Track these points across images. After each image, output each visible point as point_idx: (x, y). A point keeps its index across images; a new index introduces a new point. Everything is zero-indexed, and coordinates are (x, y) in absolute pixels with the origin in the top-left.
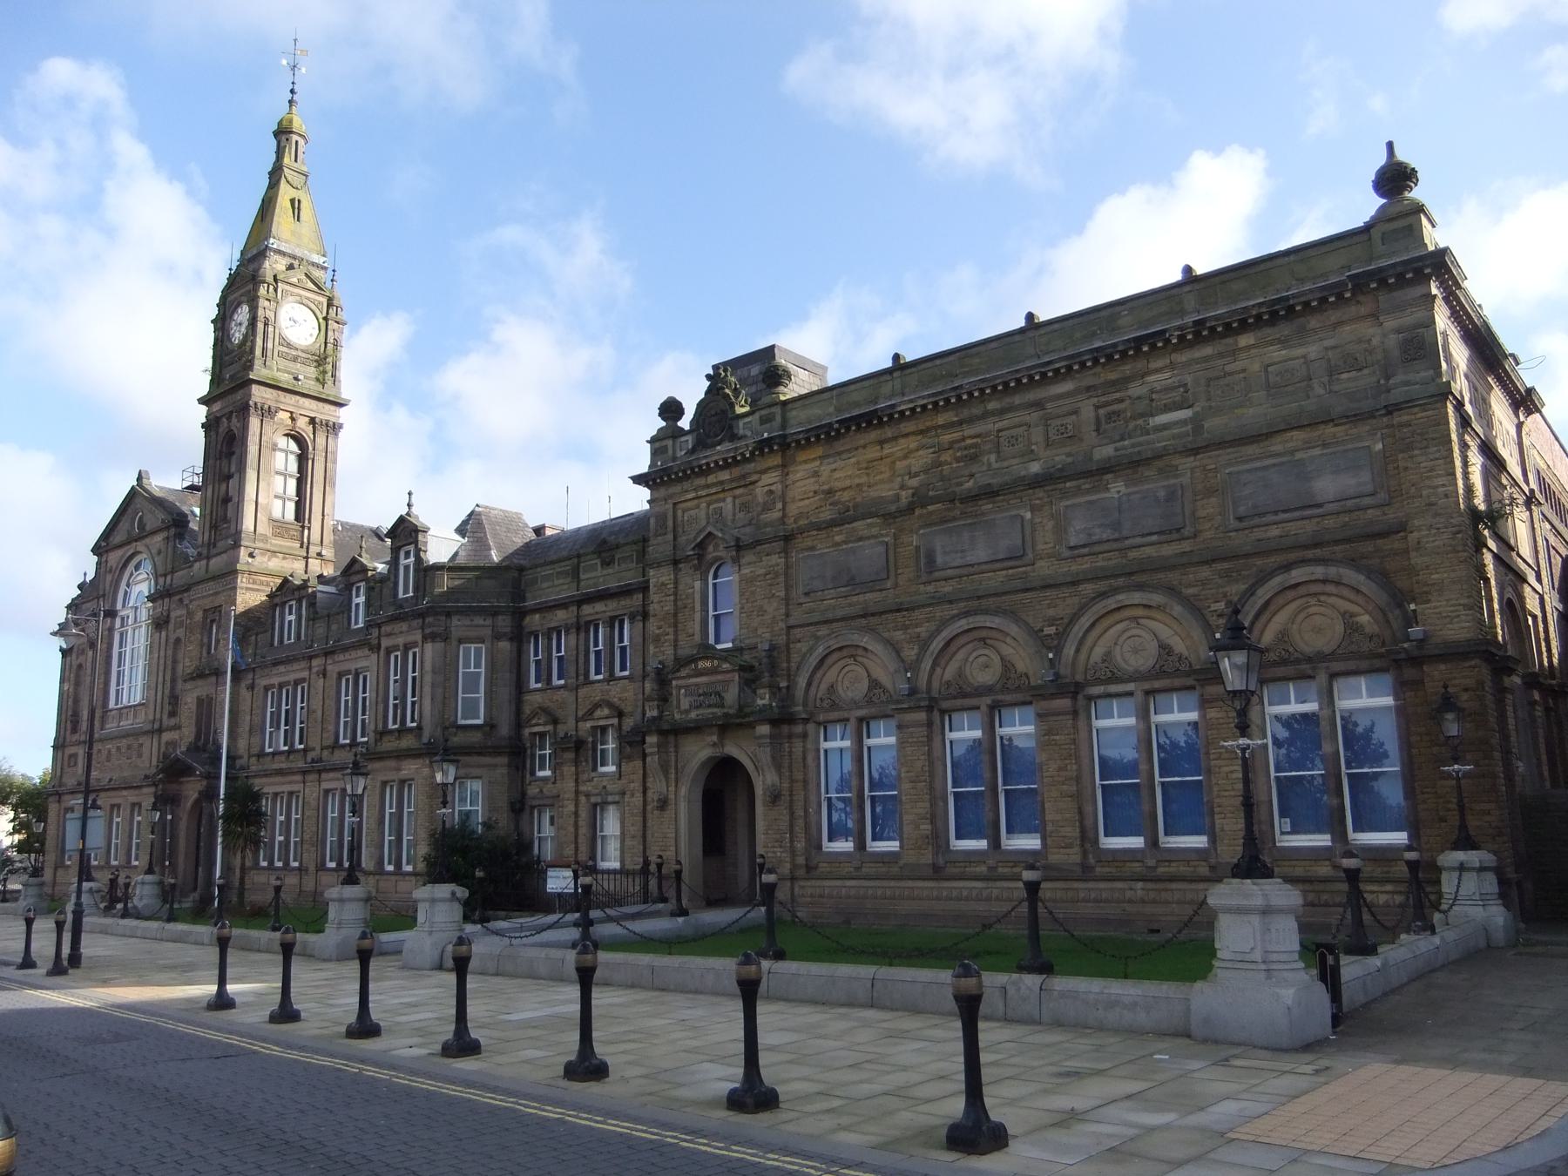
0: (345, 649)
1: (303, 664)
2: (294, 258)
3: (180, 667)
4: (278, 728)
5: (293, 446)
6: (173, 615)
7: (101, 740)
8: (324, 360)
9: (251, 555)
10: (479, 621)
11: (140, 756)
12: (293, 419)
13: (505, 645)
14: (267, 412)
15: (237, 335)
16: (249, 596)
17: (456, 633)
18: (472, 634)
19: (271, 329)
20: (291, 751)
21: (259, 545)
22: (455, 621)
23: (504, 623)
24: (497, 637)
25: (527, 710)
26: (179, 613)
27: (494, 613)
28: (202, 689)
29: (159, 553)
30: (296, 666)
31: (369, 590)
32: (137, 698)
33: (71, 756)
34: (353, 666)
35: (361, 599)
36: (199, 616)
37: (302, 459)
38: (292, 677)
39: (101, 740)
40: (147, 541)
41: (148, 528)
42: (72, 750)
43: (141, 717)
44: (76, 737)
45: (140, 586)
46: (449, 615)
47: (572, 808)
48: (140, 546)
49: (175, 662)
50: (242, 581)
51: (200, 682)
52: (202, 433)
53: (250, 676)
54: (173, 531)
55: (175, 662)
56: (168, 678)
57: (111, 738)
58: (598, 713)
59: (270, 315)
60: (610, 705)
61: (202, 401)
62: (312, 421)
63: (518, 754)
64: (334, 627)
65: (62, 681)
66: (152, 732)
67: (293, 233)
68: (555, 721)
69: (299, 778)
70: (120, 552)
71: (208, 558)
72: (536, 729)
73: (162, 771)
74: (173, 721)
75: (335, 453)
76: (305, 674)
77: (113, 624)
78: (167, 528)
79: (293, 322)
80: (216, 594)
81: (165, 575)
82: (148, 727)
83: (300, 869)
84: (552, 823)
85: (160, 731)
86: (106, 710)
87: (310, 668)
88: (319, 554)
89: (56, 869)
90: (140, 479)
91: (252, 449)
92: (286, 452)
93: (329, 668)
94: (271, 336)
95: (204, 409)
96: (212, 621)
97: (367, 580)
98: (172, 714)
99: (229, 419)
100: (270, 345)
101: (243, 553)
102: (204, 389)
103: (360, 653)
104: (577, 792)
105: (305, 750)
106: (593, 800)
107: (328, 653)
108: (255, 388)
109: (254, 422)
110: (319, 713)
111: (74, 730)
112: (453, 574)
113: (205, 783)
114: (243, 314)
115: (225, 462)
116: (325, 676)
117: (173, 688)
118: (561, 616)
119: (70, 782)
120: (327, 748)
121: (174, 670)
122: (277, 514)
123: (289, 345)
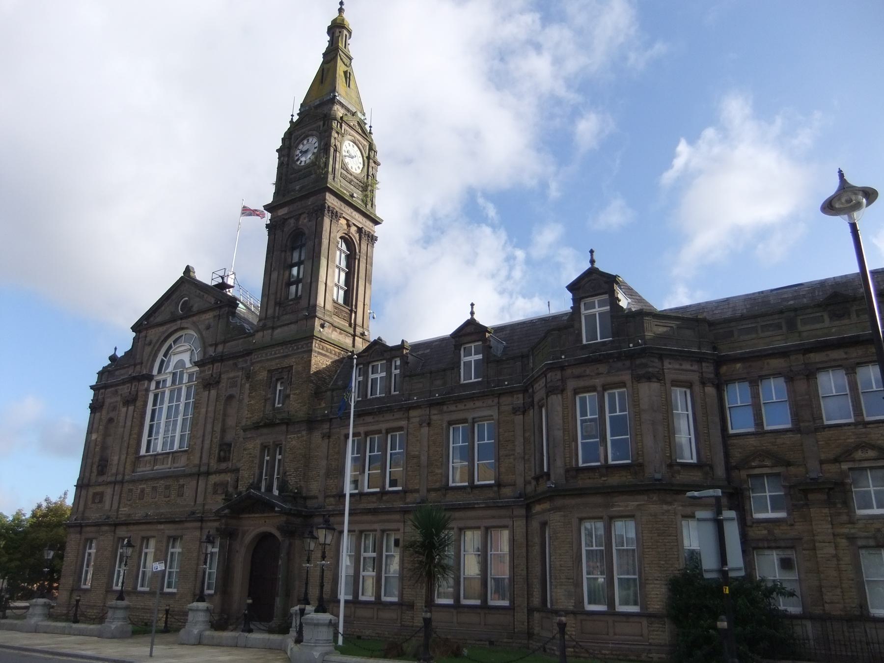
0: (460, 400)
1: (397, 415)
2: (348, 110)
3: (231, 422)
4: (364, 472)
5: (344, 247)
6: (224, 377)
7: (133, 481)
8: (367, 186)
9: (322, 326)
10: (687, 366)
11: (180, 495)
12: (349, 226)
13: (710, 390)
14: (335, 216)
15: (305, 160)
16: (320, 361)
17: (669, 377)
18: (682, 377)
19: (338, 154)
20: (383, 493)
21: (327, 318)
22: (667, 364)
23: (708, 369)
24: (703, 383)
25: (737, 455)
26: (232, 375)
27: (699, 359)
28: (269, 437)
29: (208, 328)
30: (388, 416)
31: (486, 349)
32: (176, 447)
33: (95, 494)
34: (470, 416)
35: (474, 358)
36: (263, 375)
37: (351, 258)
38: (383, 426)
39: (133, 481)
40: (195, 319)
41: (195, 309)
42: (99, 489)
43: (183, 461)
44: (101, 479)
45: (183, 355)
46: (661, 357)
47: (832, 551)
48: (185, 323)
49: (225, 415)
50: (316, 345)
51: (265, 431)
52: (265, 232)
53: (326, 426)
54: (226, 310)
55: (225, 415)
56: (218, 428)
57: (143, 480)
58: (859, 454)
59: (338, 144)
60: (873, 447)
61: (268, 208)
62: (360, 230)
63: (737, 498)
64: (438, 382)
65: (90, 432)
66: (199, 474)
67: (347, 94)
68: (788, 464)
69: (397, 517)
70: (162, 329)
71: (273, 328)
72: (757, 471)
73: (228, 507)
74: (223, 466)
75: (372, 258)
76: (403, 423)
77: (149, 386)
78: (220, 307)
79: (350, 156)
80: (286, 356)
81: (216, 345)
82: (195, 470)
83: (400, 604)
84: (786, 564)
85: (208, 474)
86: (138, 458)
87: (408, 419)
88: (363, 334)
89: (72, 591)
90: (188, 270)
91: (325, 242)
92: (341, 250)
93: (434, 418)
94: (338, 159)
95: (268, 215)
96: (277, 380)
97: (485, 340)
98: (221, 460)
99: (298, 220)
100: (337, 166)
101: (317, 323)
102: (269, 199)
103: (478, 404)
104: (834, 535)
105: (405, 492)
106: (860, 543)
107: (432, 404)
108: (329, 196)
109: (327, 221)
110: (424, 458)
111: (102, 472)
112: (655, 322)
113: (284, 518)
114: (311, 144)
115: (288, 254)
116: (429, 424)
117: (222, 438)
118: (777, 363)
119: (94, 515)
120: (435, 490)
121: (224, 421)
122: (335, 298)
123: (347, 170)
